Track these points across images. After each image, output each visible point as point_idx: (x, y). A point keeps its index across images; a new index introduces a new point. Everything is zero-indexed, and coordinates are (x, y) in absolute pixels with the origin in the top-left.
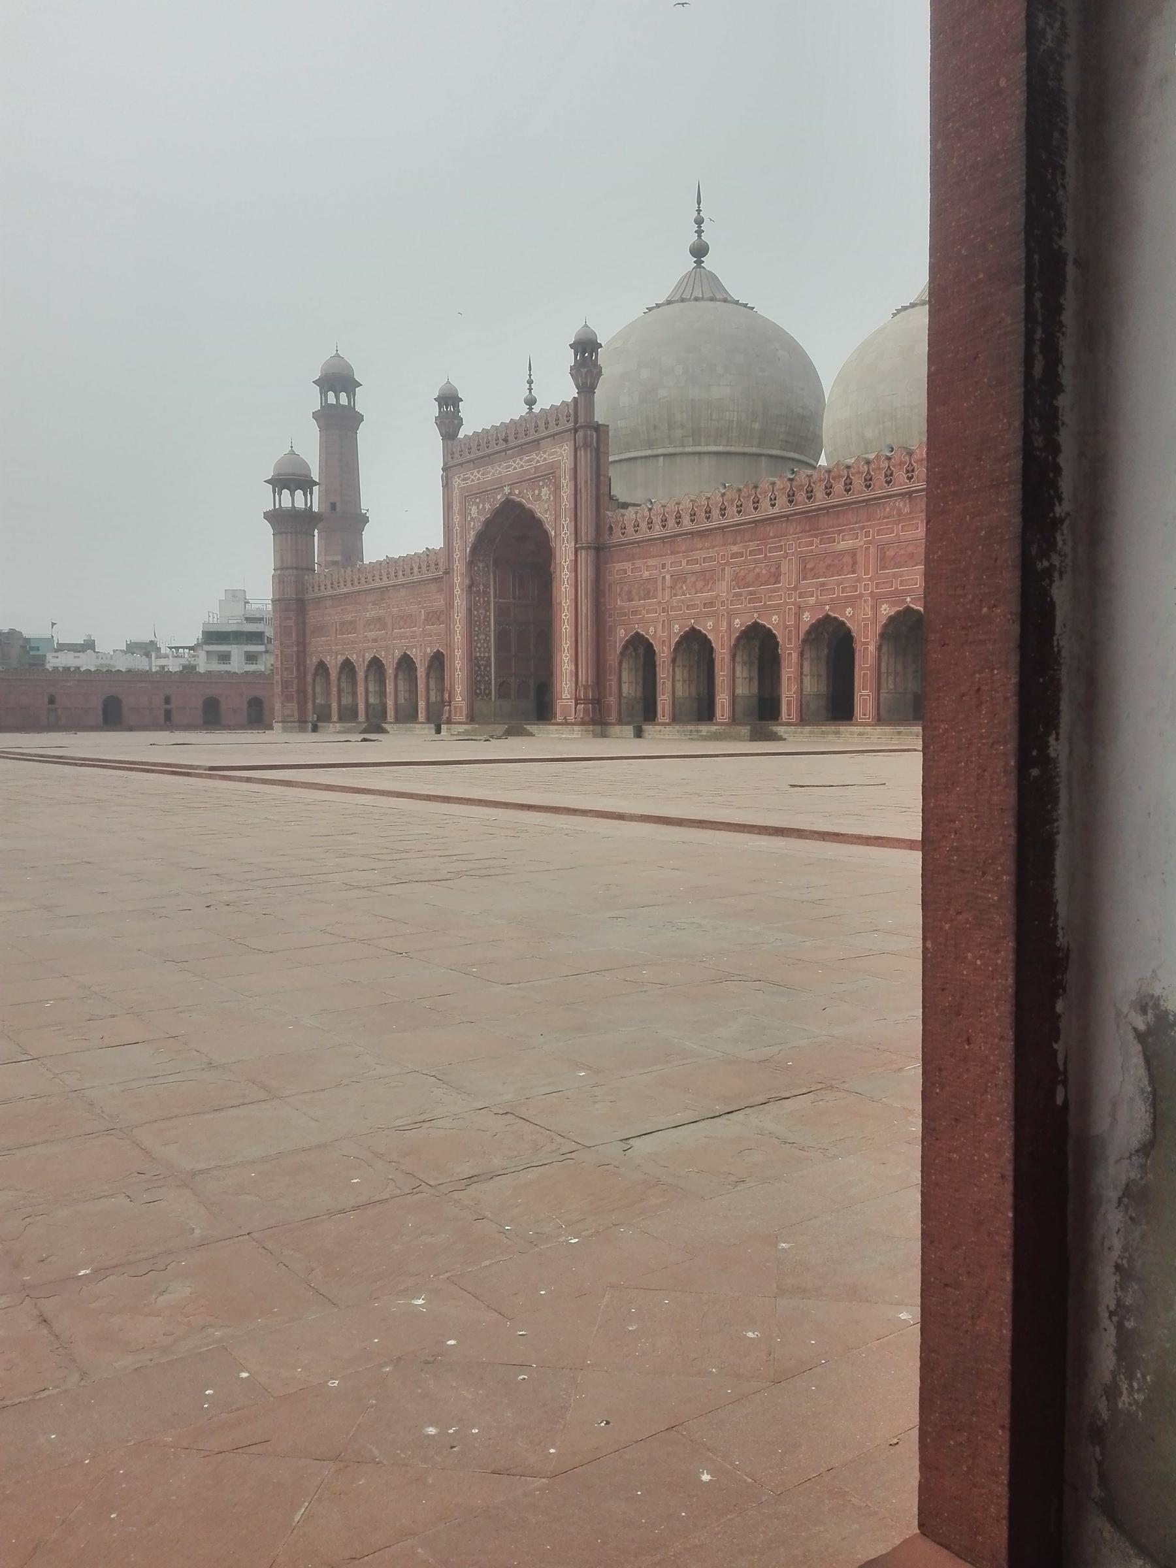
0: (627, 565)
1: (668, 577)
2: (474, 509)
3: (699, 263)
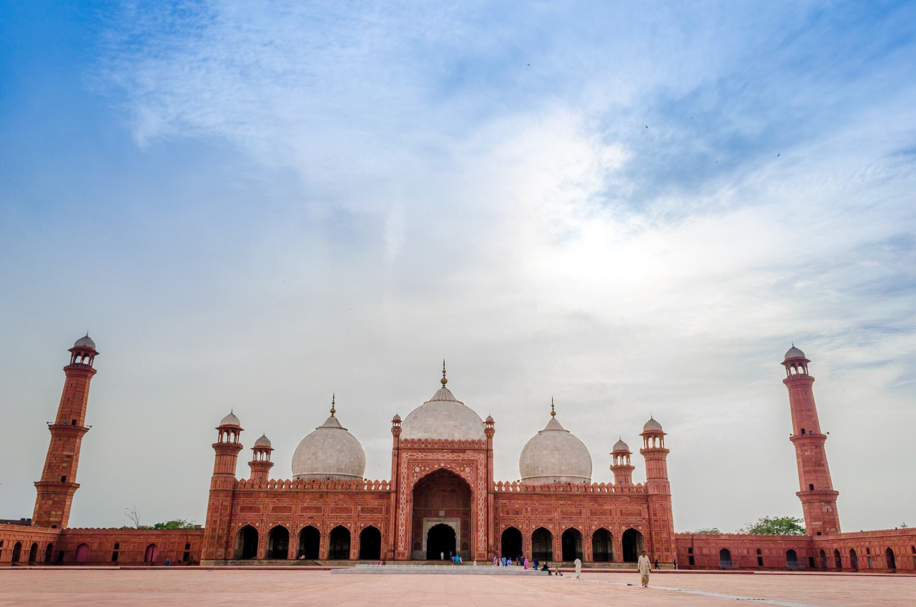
2: (417, 469)
3: (444, 386)
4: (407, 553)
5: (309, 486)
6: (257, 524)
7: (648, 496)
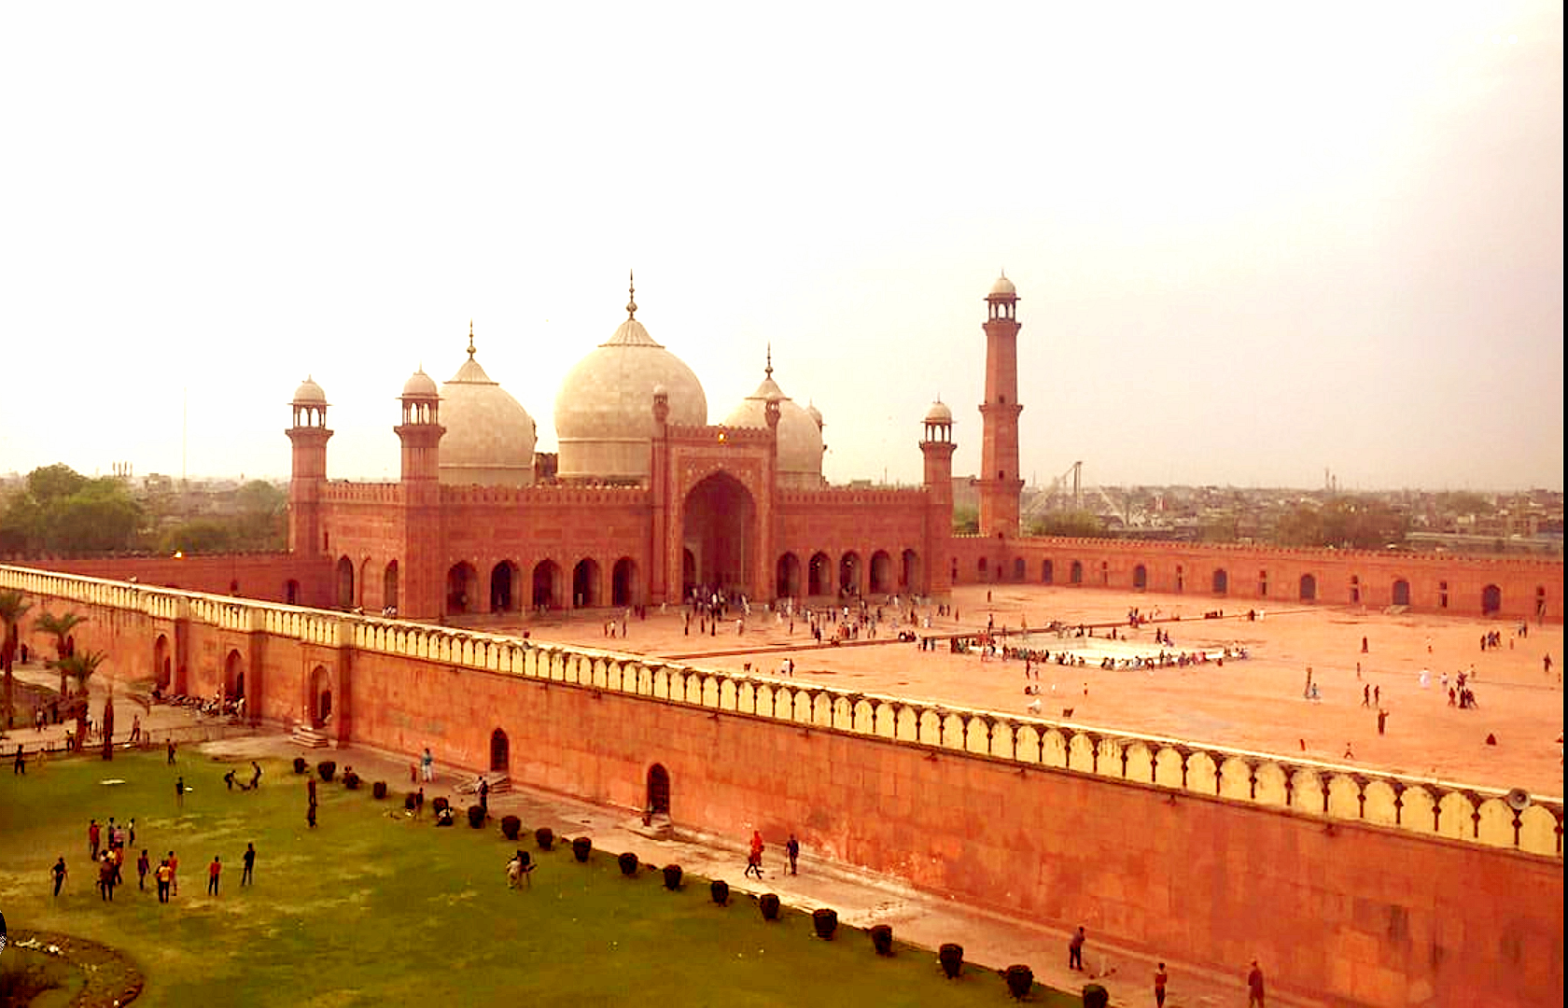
4: (680, 594)
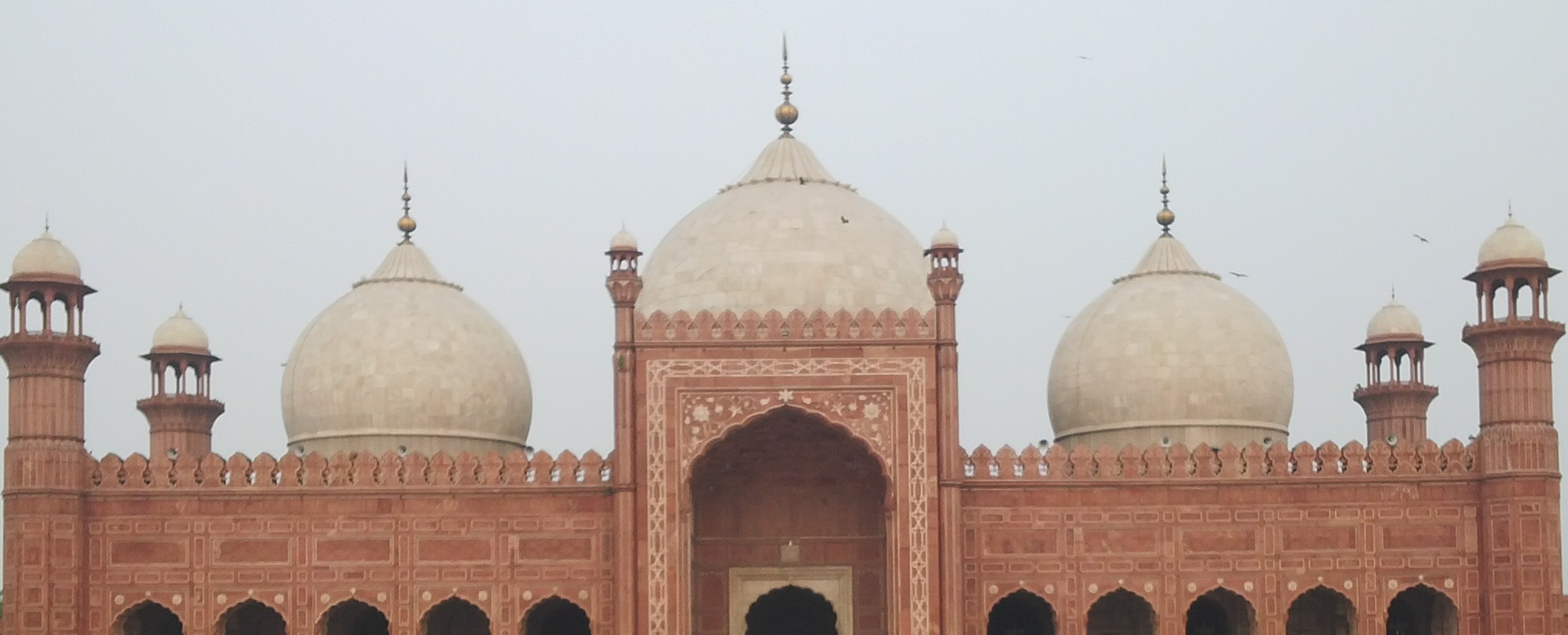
0: (1005, 511)
1: (1078, 532)
2: (701, 413)
5: (342, 474)
6: (177, 599)
7: (1481, 481)
